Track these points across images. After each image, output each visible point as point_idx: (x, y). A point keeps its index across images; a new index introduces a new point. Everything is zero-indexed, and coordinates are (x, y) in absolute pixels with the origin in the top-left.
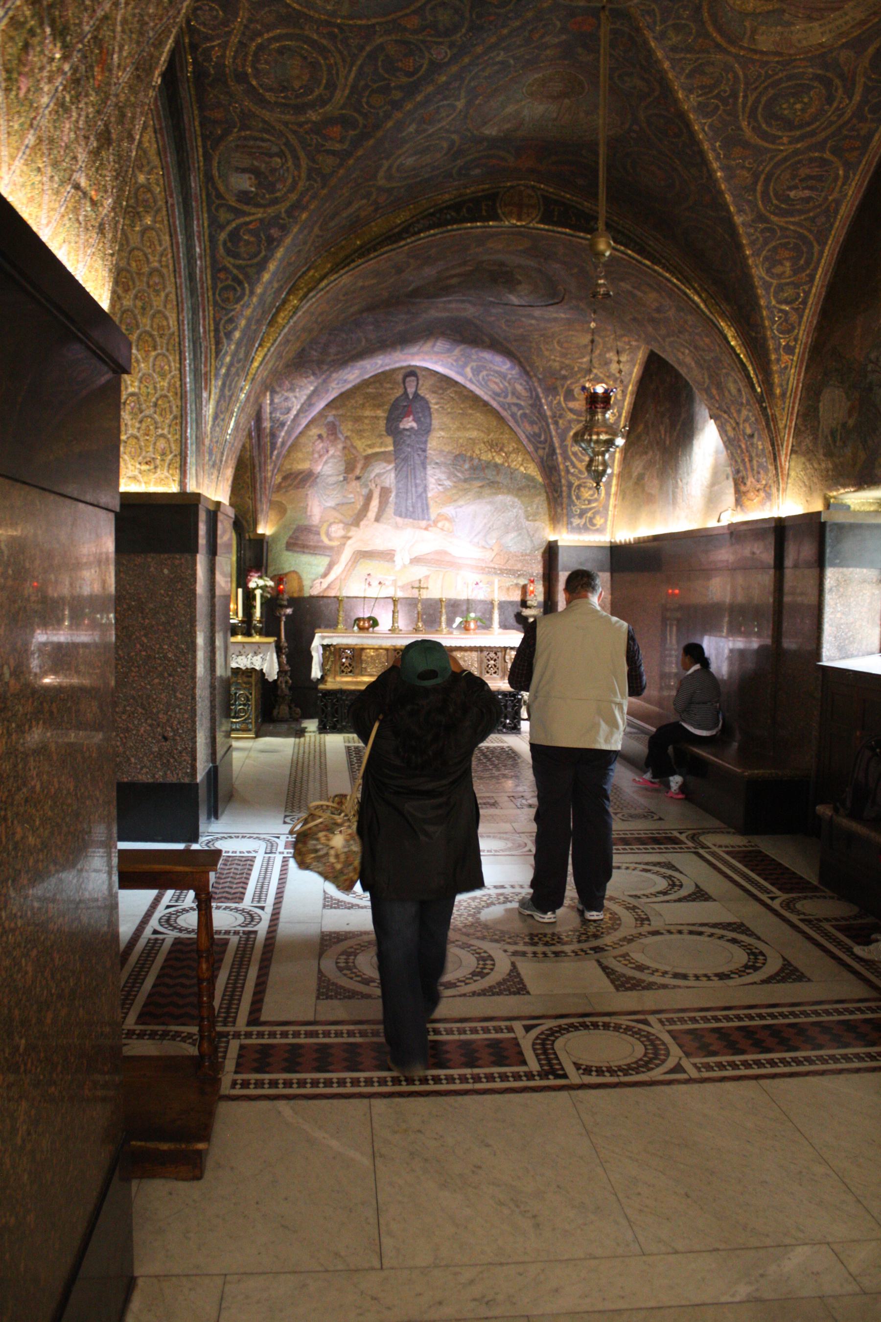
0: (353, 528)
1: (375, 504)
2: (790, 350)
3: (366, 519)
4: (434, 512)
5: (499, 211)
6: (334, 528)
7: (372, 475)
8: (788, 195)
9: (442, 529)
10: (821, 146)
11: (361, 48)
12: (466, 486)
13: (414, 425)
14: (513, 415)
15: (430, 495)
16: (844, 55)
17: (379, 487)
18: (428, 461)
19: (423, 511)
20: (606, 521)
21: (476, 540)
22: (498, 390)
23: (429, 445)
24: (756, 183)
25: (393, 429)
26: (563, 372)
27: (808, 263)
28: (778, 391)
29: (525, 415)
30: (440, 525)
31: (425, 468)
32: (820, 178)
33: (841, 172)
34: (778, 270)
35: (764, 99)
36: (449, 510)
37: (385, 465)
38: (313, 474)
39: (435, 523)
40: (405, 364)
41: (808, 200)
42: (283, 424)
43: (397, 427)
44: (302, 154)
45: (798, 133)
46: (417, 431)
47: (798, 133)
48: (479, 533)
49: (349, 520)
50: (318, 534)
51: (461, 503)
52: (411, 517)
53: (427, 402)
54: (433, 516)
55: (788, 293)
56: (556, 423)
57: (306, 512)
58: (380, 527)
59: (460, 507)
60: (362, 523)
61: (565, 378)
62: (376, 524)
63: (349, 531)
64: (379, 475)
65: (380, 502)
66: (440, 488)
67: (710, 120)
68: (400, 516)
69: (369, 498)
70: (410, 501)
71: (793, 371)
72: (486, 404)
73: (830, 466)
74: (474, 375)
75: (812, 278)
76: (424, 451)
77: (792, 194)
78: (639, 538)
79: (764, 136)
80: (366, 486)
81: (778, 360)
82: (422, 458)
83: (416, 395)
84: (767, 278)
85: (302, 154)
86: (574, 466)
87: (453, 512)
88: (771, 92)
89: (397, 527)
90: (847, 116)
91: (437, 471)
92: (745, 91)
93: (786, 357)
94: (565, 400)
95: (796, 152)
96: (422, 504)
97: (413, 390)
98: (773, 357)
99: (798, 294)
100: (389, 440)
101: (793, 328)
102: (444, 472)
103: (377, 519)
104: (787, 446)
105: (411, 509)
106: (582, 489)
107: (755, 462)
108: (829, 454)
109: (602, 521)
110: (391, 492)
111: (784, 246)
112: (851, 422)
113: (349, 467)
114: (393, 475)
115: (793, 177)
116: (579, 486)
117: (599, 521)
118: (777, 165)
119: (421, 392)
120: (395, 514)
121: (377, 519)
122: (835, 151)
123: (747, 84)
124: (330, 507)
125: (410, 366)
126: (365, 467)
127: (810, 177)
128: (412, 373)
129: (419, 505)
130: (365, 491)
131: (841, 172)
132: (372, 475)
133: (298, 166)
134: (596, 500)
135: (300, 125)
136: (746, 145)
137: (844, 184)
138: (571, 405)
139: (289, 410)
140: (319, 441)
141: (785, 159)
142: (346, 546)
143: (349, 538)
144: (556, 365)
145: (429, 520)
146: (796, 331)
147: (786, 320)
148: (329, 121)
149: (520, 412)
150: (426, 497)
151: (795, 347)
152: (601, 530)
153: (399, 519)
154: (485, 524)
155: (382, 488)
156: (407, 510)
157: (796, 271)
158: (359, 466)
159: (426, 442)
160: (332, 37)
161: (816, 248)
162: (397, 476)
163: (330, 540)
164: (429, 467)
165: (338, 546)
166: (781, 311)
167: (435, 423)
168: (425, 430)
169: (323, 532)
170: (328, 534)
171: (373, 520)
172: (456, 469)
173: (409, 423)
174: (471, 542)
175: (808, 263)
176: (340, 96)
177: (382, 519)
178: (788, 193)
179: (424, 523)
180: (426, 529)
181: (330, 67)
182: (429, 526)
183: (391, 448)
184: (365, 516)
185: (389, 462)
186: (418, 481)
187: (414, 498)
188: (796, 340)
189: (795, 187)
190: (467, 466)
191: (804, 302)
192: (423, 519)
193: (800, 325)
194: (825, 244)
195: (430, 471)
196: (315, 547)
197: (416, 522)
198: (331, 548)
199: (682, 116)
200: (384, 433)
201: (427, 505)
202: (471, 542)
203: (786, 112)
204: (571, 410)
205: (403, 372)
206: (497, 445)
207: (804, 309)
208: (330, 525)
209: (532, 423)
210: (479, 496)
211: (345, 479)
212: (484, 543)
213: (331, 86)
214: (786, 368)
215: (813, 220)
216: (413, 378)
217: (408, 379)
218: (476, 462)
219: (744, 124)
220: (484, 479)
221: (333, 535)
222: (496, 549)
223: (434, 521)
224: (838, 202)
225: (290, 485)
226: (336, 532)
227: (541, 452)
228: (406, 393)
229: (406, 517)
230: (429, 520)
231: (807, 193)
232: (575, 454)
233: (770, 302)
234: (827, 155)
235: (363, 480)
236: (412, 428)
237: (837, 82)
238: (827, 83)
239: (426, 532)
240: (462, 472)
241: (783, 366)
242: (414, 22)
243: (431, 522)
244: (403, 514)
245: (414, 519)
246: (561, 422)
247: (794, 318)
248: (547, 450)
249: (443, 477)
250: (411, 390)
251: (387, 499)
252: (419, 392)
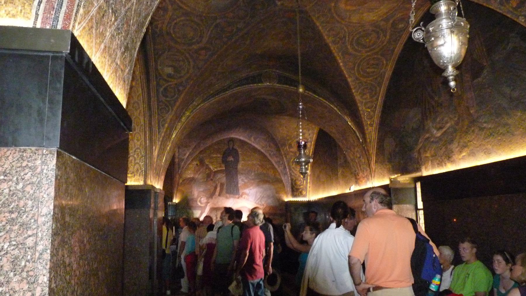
1: (218, 189)
2: (371, 125)
4: (241, 191)
5: (263, 80)
6: (202, 199)
7: (218, 178)
8: (366, 71)
10: (376, 53)
11: (212, 24)
12: (253, 181)
13: (232, 159)
14: (270, 155)
15: (239, 185)
16: (382, 23)
19: (237, 191)
20: (306, 193)
21: (257, 202)
22: (264, 145)
24: (354, 67)
25: (224, 161)
26: (288, 138)
27: (375, 94)
28: (368, 140)
29: (274, 154)
30: (243, 196)
31: (237, 176)
32: (377, 65)
33: (385, 62)
34: (365, 97)
35: (355, 38)
36: (247, 191)
39: (242, 196)
40: (229, 137)
41: (374, 72)
42: (183, 160)
44: (191, 60)
45: (368, 49)
47: (368, 49)
48: (258, 199)
51: (251, 188)
52: (232, 194)
53: (237, 151)
54: (241, 194)
55: (369, 105)
56: (286, 157)
57: (192, 193)
58: (221, 198)
59: (251, 189)
60: (213, 197)
61: (288, 140)
62: (219, 197)
67: (337, 46)
69: (216, 188)
71: (373, 133)
72: (259, 151)
73: (391, 166)
74: (254, 140)
75: (377, 100)
77: (368, 70)
78: (319, 199)
79: (356, 50)
81: (367, 129)
83: (233, 148)
84: (361, 100)
85: (191, 60)
86: (294, 173)
88: (358, 36)
89: (227, 198)
90: (385, 43)
92: (349, 36)
93: (370, 128)
94: (289, 148)
95: (368, 56)
98: (366, 128)
99: (373, 105)
100: (223, 165)
101: (372, 118)
104: (374, 160)
106: (297, 181)
107: (362, 168)
108: (390, 161)
109: (305, 193)
111: (367, 88)
112: (397, 150)
113: (208, 176)
114: (225, 178)
115: (368, 64)
116: (295, 180)
117: (304, 193)
118: (361, 61)
119: (235, 147)
121: (219, 195)
122: (382, 55)
123: (349, 33)
124: (201, 191)
125: (230, 138)
126: (214, 175)
127: (373, 64)
128: (232, 140)
130: (214, 185)
131: (385, 62)
132: (218, 178)
133: (189, 65)
134: (302, 185)
135: (190, 50)
136: (350, 54)
137: (386, 66)
138: (291, 150)
139: (185, 155)
141: (364, 59)
144: (285, 135)
146: (373, 118)
147: (369, 114)
148: (201, 49)
150: (238, 187)
151: (373, 124)
152: (305, 196)
154: (261, 196)
157: (371, 97)
158: (212, 176)
160: (202, 20)
161: (378, 89)
162: (226, 179)
163: (201, 203)
164: (238, 175)
166: (367, 111)
167: (240, 159)
168: (237, 161)
170: (200, 201)
171: (217, 196)
173: (231, 159)
175: (375, 94)
176: (205, 40)
178: (366, 70)
179: (237, 196)
180: (238, 198)
181: (201, 31)
183: (224, 168)
186: (234, 180)
188: (373, 122)
189: (369, 68)
190: (253, 174)
191: (376, 107)
192: (237, 194)
193: (374, 115)
194: (381, 87)
195: (239, 176)
199: (326, 45)
203: (363, 42)
204: (291, 152)
207: (376, 110)
209: (277, 157)
210: (258, 185)
211: (207, 180)
212: (260, 203)
213: (201, 37)
214: (371, 132)
215: (376, 79)
216: (232, 142)
219: (349, 47)
221: (202, 202)
222: (265, 205)
224: (385, 73)
226: (203, 200)
227: (280, 168)
228: (229, 148)
230: (239, 194)
231: (373, 70)
232: (293, 168)
233: (363, 108)
234: (379, 56)
236: (231, 161)
237: (380, 32)
238: (378, 33)
241: (369, 131)
242: (231, 15)
246: (288, 156)
247: (372, 113)
248: (283, 167)
249: (244, 178)
250: (231, 147)
251: (223, 188)
252: (234, 147)
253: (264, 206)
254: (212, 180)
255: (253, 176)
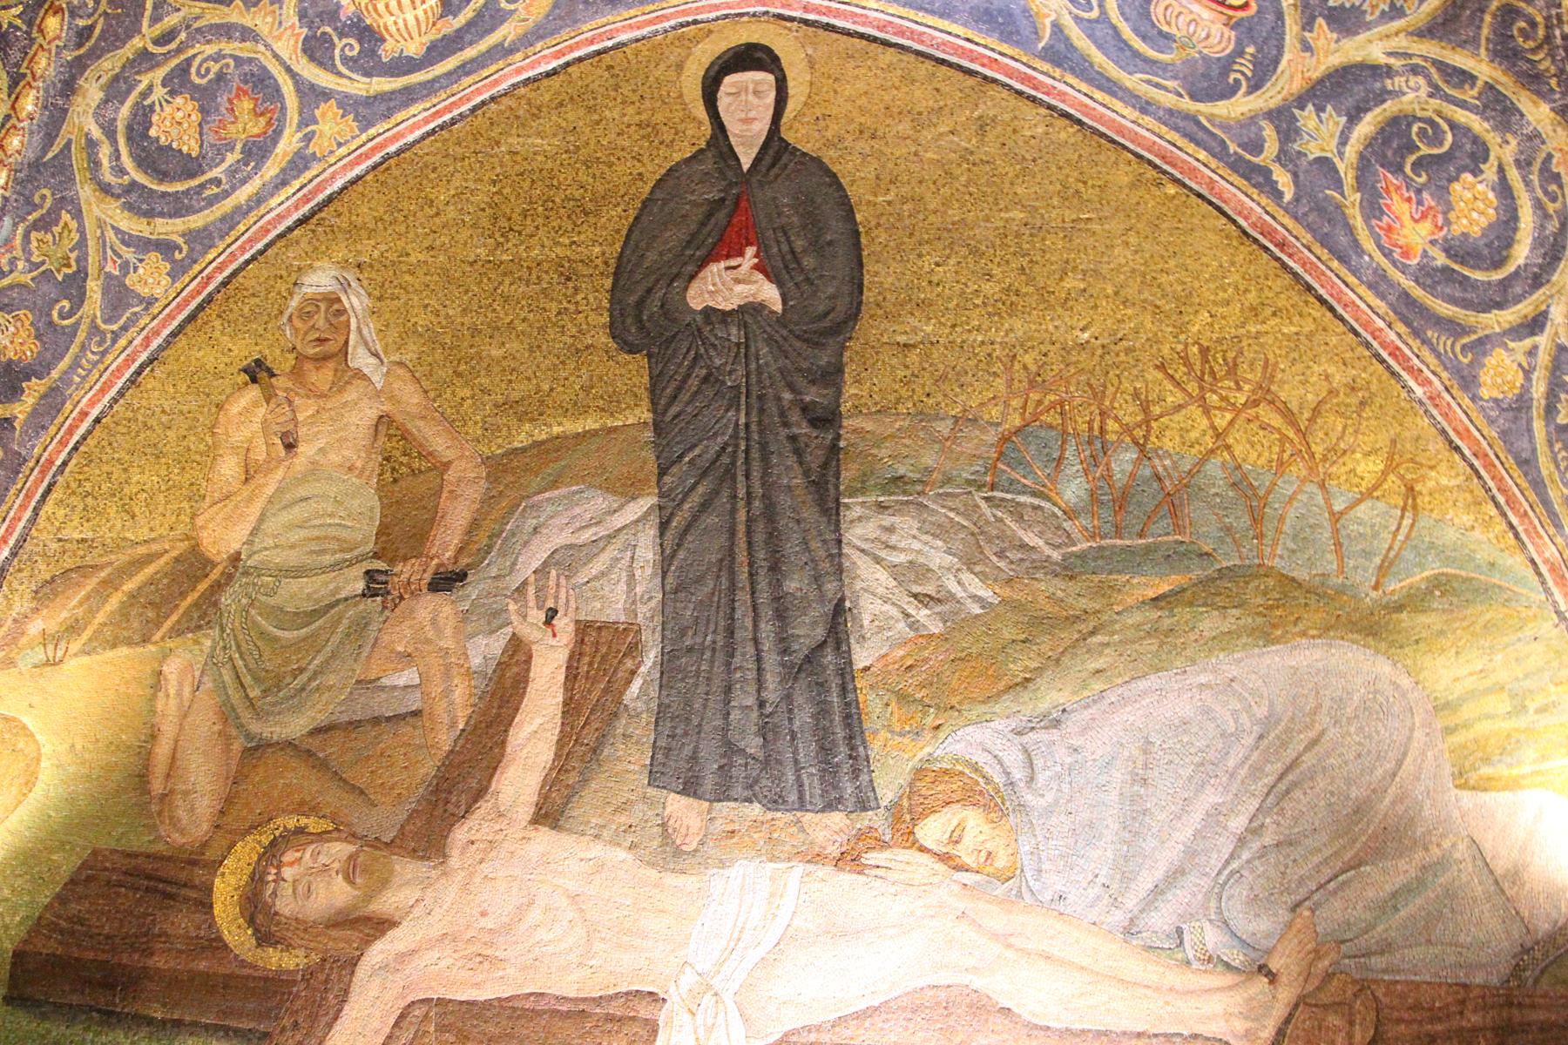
0: (406, 869)
3: (484, 807)
9: (944, 858)
13: (770, 294)
17: (564, 624)
18: (848, 474)
19: (825, 750)
21: (1161, 920)
23: (850, 390)
30: (932, 831)
31: (831, 510)
37: (599, 502)
38: (208, 563)
43: (672, 311)
46: (782, 320)
48: (1176, 875)
49: (386, 819)
50: (208, 907)
51: (1050, 696)
54: (889, 783)
60: (460, 834)
62: (544, 838)
63: (384, 883)
64: (566, 560)
65: (570, 708)
66: (922, 614)
68: (690, 788)
70: (745, 698)
76: (827, 419)
80: (495, 620)
82: (814, 458)
87: (1013, 758)
91: (906, 523)
96: (822, 711)
97: (762, 127)
102: (941, 531)
103: (548, 814)
105: (753, 745)
110: (635, 649)
120: (655, 776)
121: (548, 814)
129: (804, 717)
130: (486, 649)
140: (254, 392)
142: (362, 971)
143: (382, 925)
145: (863, 805)
149: (1367, 126)
150: (846, 672)
153: (683, 810)
155: (583, 628)
156: (730, 749)
159: (832, 376)
162: (665, 562)
163: (265, 938)
164: (854, 507)
165: (309, 974)
169: (226, 889)
170: (254, 906)
171: (525, 812)
172: (1017, 512)
174: (1129, 931)
177: (576, 811)
179: (830, 828)
180: (849, 860)
182: (867, 840)
184: (480, 793)
185: (628, 489)
186: (791, 585)
187: (771, 681)
190: (1073, 490)
192: (829, 807)
196: (179, 985)
197: (782, 817)
198: (273, 987)
200: (604, 339)
201: (852, 720)
202: (1129, 931)
205: (706, 53)
206: (1232, 370)
208: (272, 852)
211: (375, 584)
212: (1213, 938)
216: (766, 79)
217: (729, 80)
218: (1123, 462)
220: (1174, 557)
221: (285, 905)
223: (895, 811)
225: (73, 628)
229: (722, 794)
235: (473, 590)
236: (752, 310)
239: (846, 878)
240: (1049, 524)
243: (875, 819)
244: (709, 782)
245: (776, 802)
249: (937, 556)
251: (615, 691)
253: (1272, 977)
254: (446, 581)
255: (1071, 514)
